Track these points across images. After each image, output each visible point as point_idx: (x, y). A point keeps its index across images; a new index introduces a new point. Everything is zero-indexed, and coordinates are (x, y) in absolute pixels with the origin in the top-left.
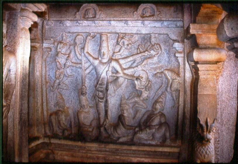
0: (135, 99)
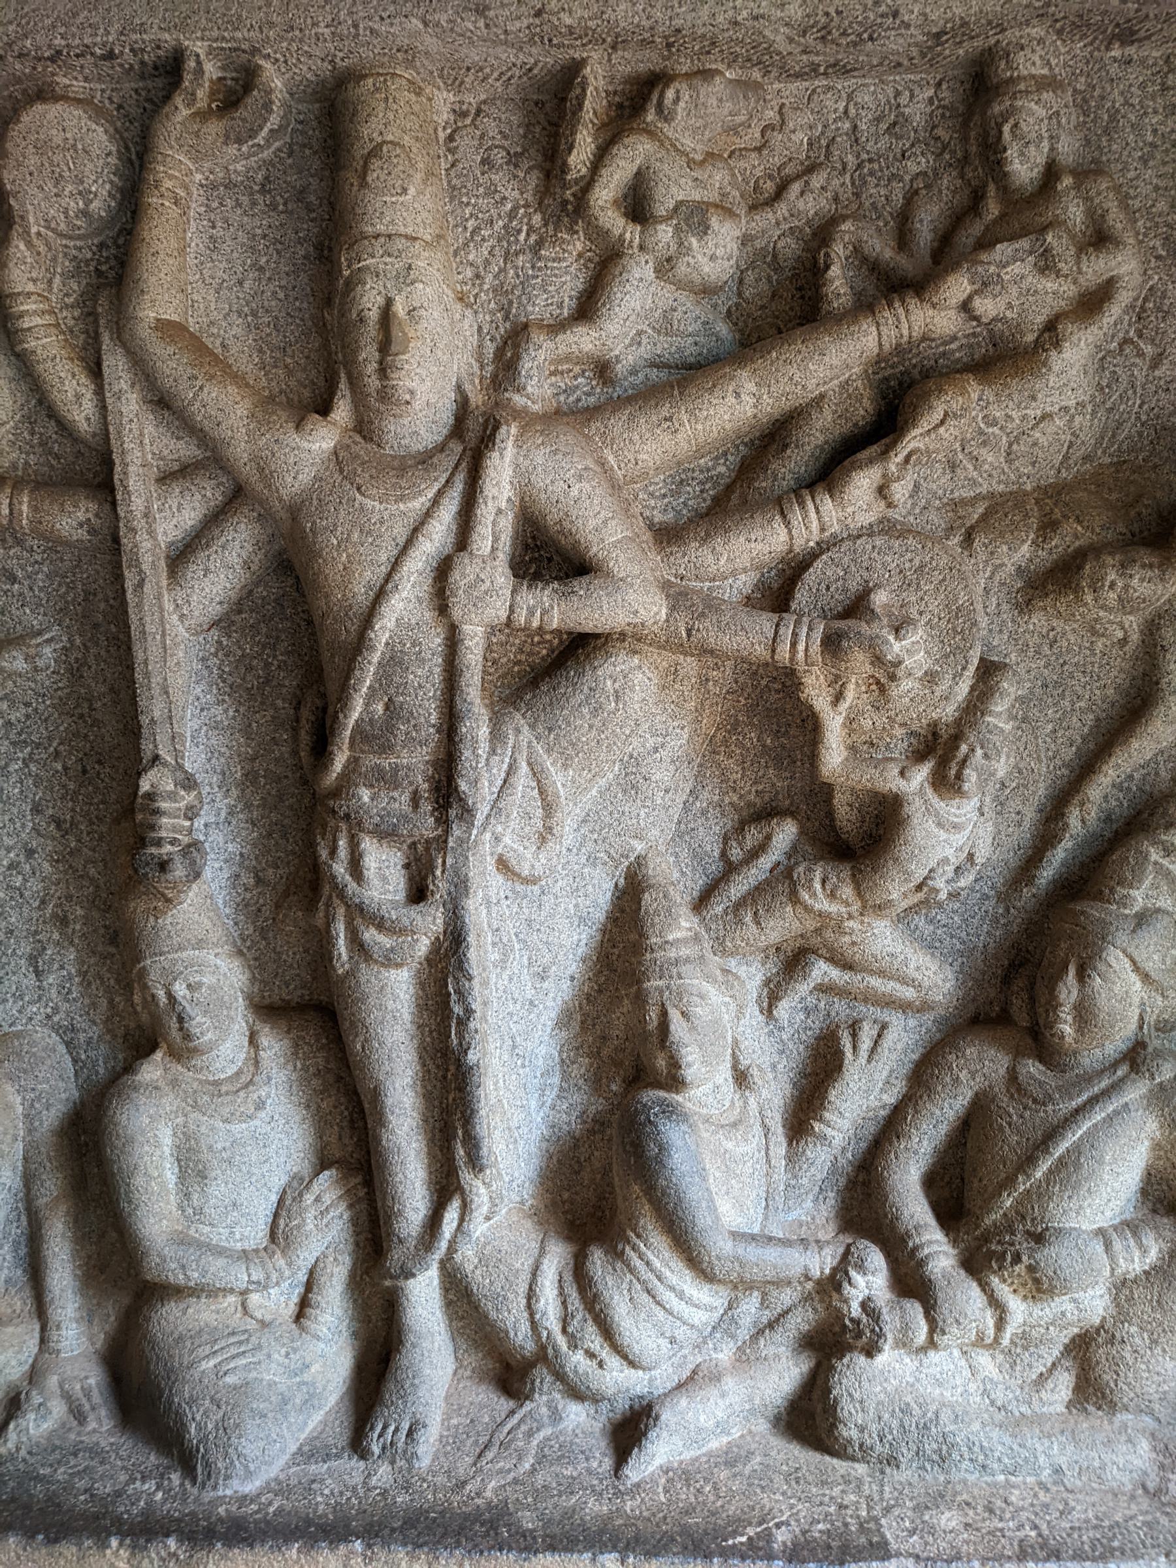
0: (805, 896)
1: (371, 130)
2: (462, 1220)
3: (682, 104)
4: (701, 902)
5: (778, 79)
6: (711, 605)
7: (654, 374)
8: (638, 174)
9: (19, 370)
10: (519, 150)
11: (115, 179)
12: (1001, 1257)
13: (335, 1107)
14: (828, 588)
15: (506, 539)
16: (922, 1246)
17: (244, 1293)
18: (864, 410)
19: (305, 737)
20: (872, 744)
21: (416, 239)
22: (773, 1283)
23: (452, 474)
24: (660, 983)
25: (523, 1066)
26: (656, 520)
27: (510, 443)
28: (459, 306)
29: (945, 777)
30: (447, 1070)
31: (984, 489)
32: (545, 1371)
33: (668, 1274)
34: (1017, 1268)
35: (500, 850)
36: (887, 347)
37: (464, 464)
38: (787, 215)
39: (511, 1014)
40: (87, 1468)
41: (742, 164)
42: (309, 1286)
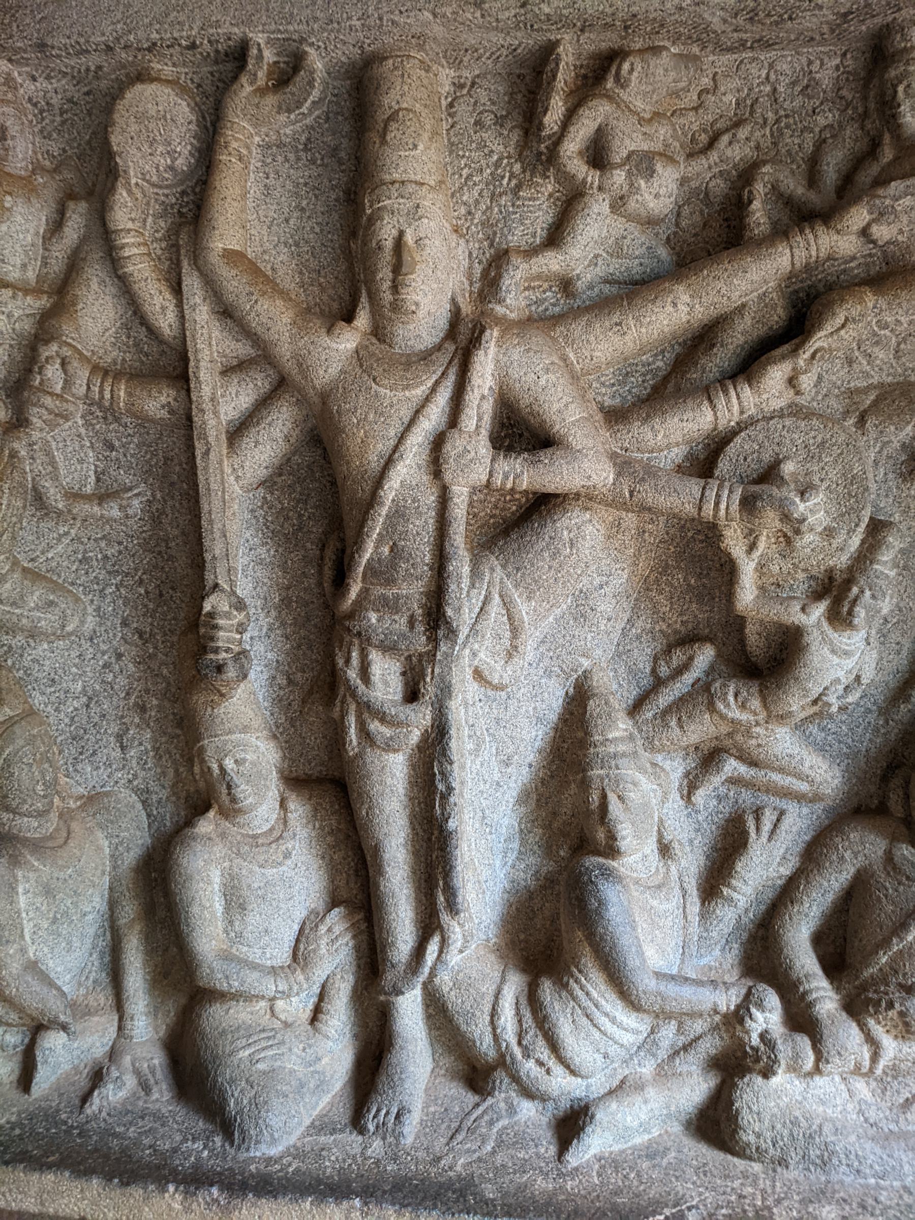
0: (720, 706)
1: (390, 100)
2: (441, 952)
3: (635, 74)
4: (635, 709)
5: (713, 53)
6: (650, 472)
7: (607, 289)
8: (599, 131)
9: (120, 288)
10: (504, 113)
11: (195, 142)
12: (877, 1003)
13: (344, 859)
14: (745, 459)
15: (487, 419)
16: (811, 991)
17: (273, 999)
18: (778, 316)
19: (328, 572)
20: (779, 585)
21: (423, 184)
22: (688, 1014)
23: (447, 368)
24: (602, 772)
25: (491, 833)
26: (606, 404)
27: (493, 344)
28: (454, 236)
29: (838, 613)
30: (432, 834)
31: (875, 380)
32: (504, 1074)
33: (604, 1003)
34: (890, 1013)
35: (476, 663)
36: (798, 265)
37: (456, 361)
38: (717, 160)
39: (482, 792)
40: (151, 1129)
41: (682, 121)
42: (322, 997)
